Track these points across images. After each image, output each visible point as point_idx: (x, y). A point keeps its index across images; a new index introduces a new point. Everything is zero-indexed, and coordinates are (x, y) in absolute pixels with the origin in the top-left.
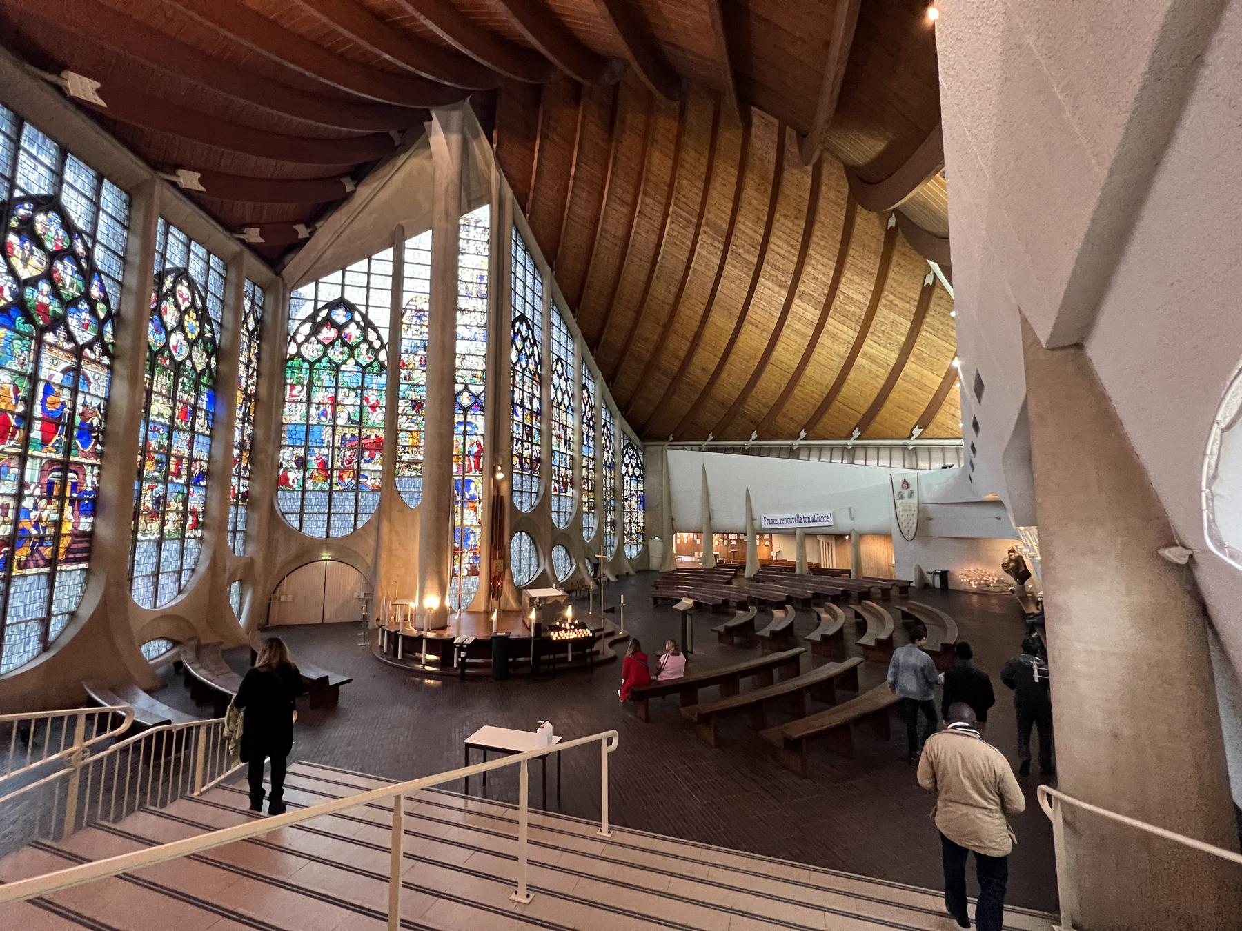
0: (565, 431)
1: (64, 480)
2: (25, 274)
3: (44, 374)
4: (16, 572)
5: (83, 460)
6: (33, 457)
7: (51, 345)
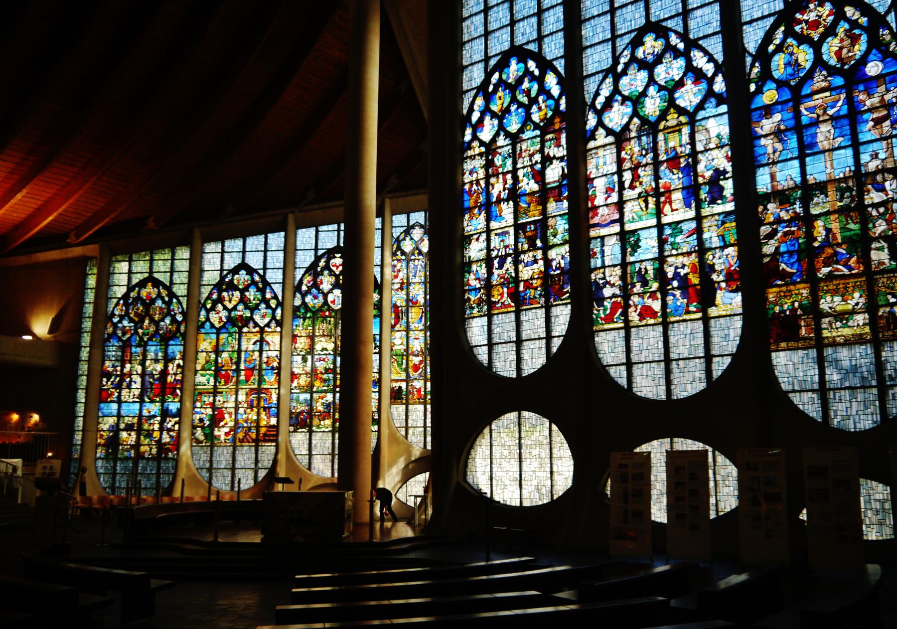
0: (691, 169)
1: (259, 399)
2: (230, 306)
3: (243, 348)
4: (238, 444)
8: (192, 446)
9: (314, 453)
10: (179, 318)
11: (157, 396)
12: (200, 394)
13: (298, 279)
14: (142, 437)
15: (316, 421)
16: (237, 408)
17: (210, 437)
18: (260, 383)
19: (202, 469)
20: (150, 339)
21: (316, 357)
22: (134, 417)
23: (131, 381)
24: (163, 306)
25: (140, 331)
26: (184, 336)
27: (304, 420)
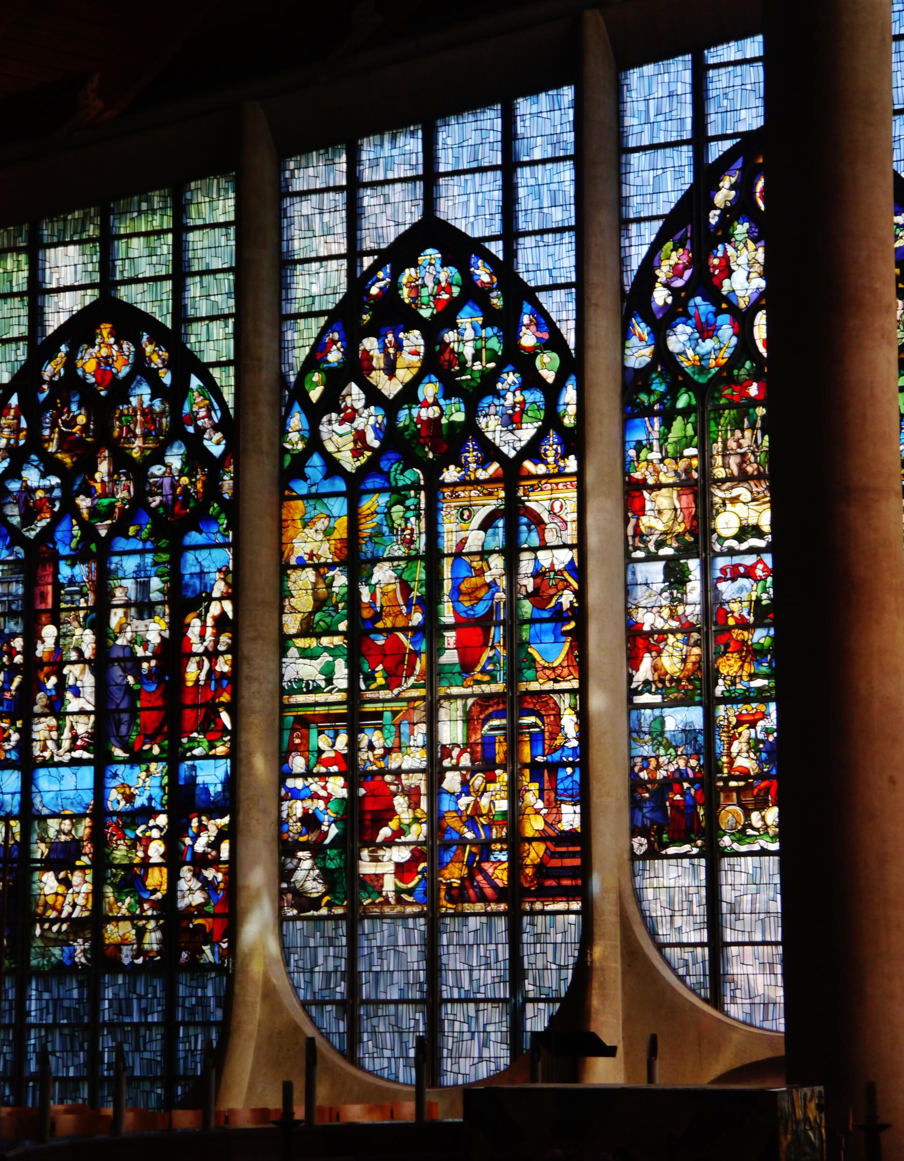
2: (390, 388)
3: (448, 543)
4: (447, 907)
5: (549, 686)
6: (449, 697)
7: (454, 485)
8: (282, 919)
9: (729, 936)
10: (215, 446)
11: (152, 738)
12: (303, 723)
13: (635, 263)
14: (109, 891)
15: (730, 815)
16: (434, 772)
17: (346, 883)
18: (513, 677)
19: (321, 1003)
20: (118, 530)
21: (721, 562)
22: (76, 818)
23: (62, 686)
24: (158, 405)
25: (84, 503)
26: (233, 510)
27: (686, 810)
